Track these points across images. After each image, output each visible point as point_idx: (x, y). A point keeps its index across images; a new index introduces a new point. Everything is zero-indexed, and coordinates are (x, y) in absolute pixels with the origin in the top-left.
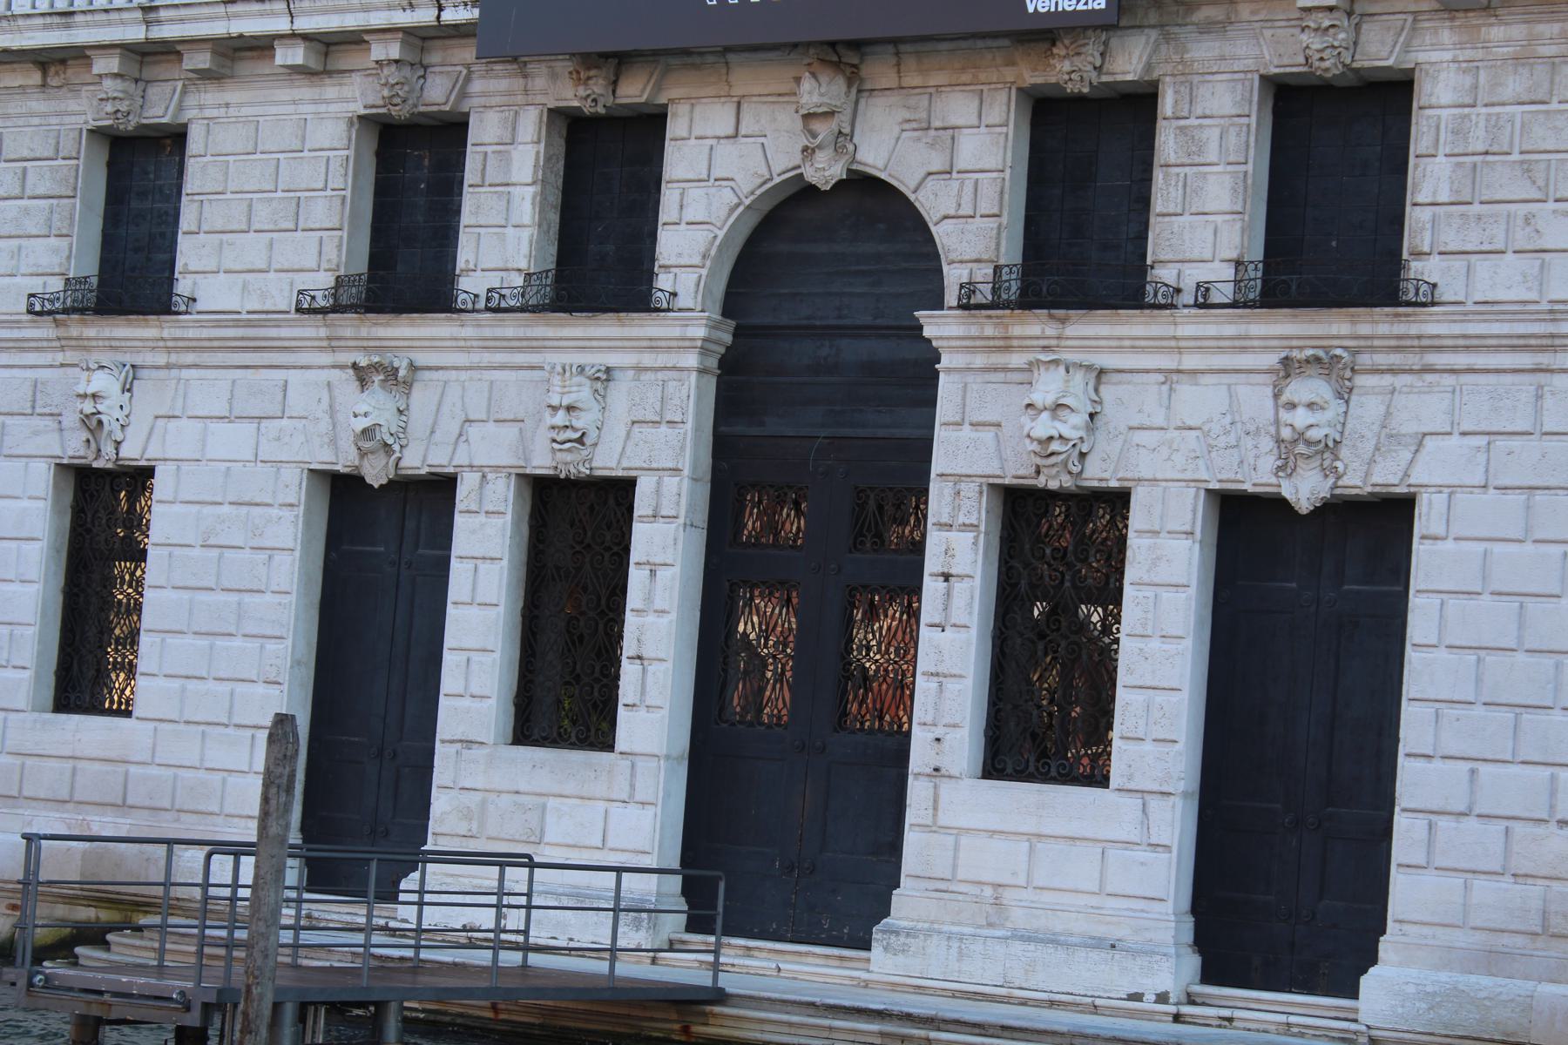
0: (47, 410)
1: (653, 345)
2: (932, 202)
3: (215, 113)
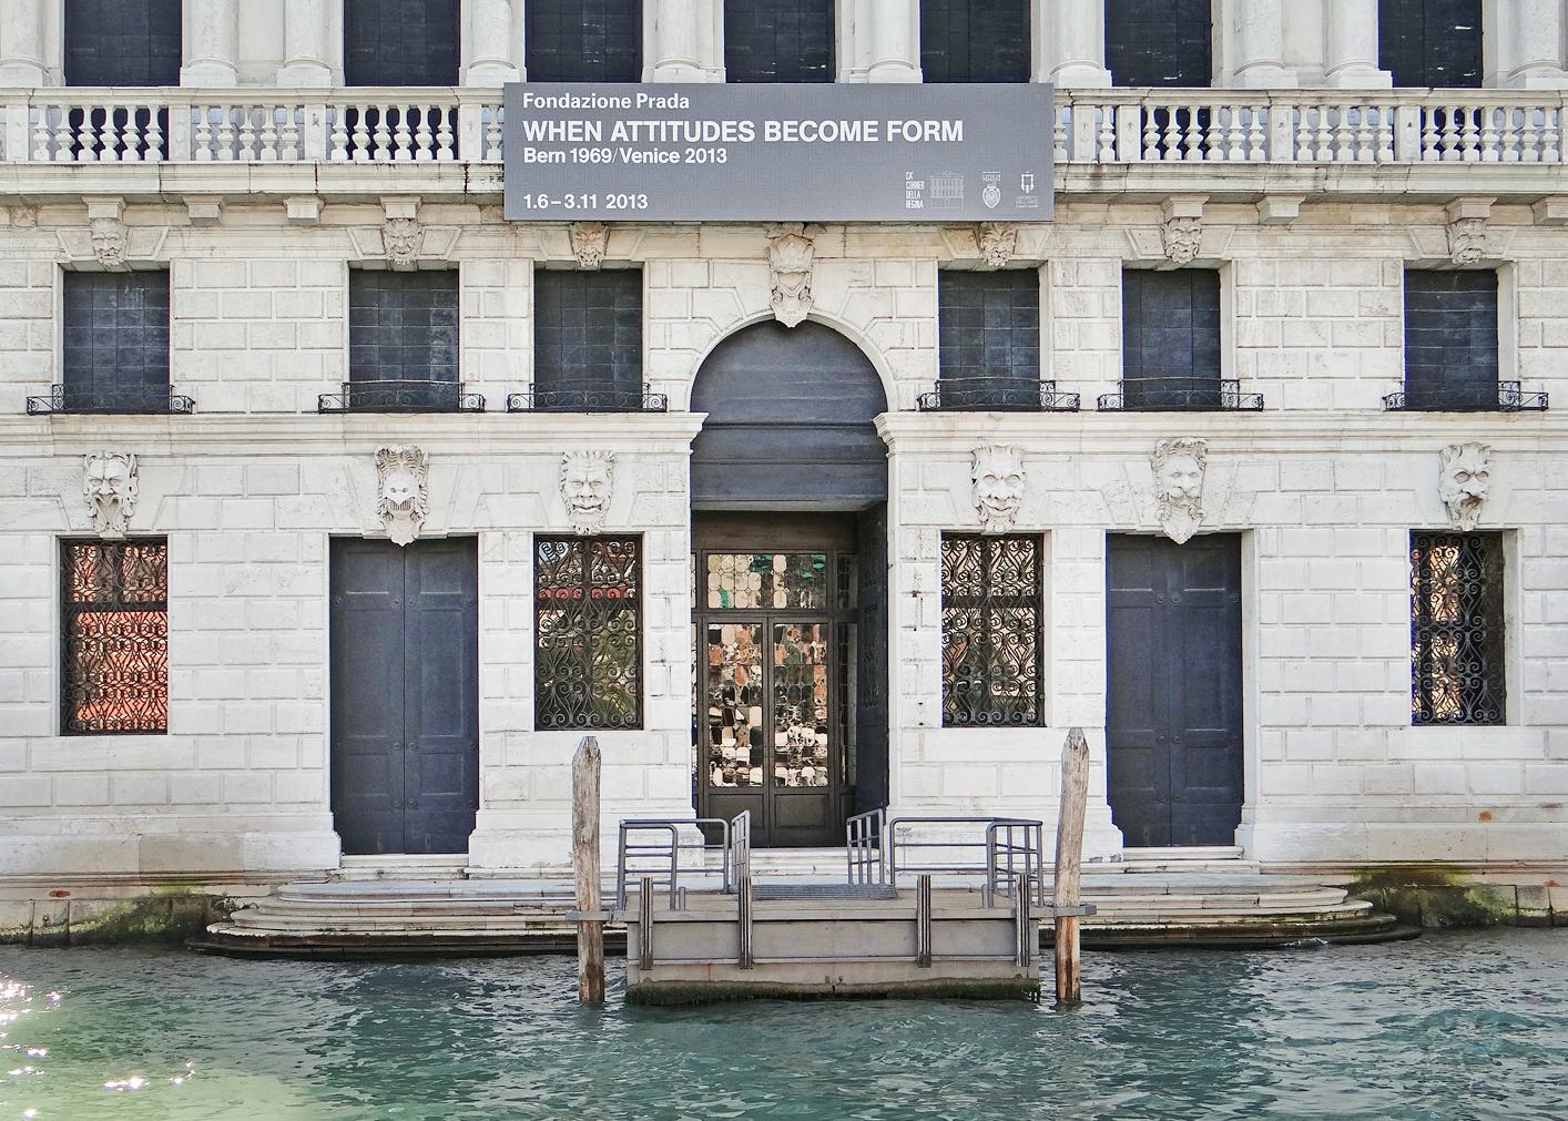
0: (44, 492)
1: (652, 437)
3: (199, 254)
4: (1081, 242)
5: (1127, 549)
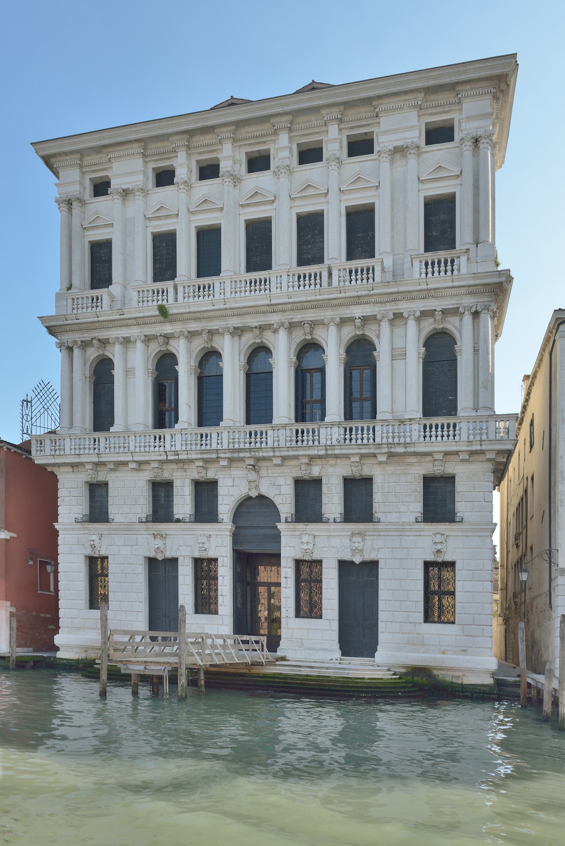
2: (277, 501)
4: (330, 470)
5: (344, 566)
